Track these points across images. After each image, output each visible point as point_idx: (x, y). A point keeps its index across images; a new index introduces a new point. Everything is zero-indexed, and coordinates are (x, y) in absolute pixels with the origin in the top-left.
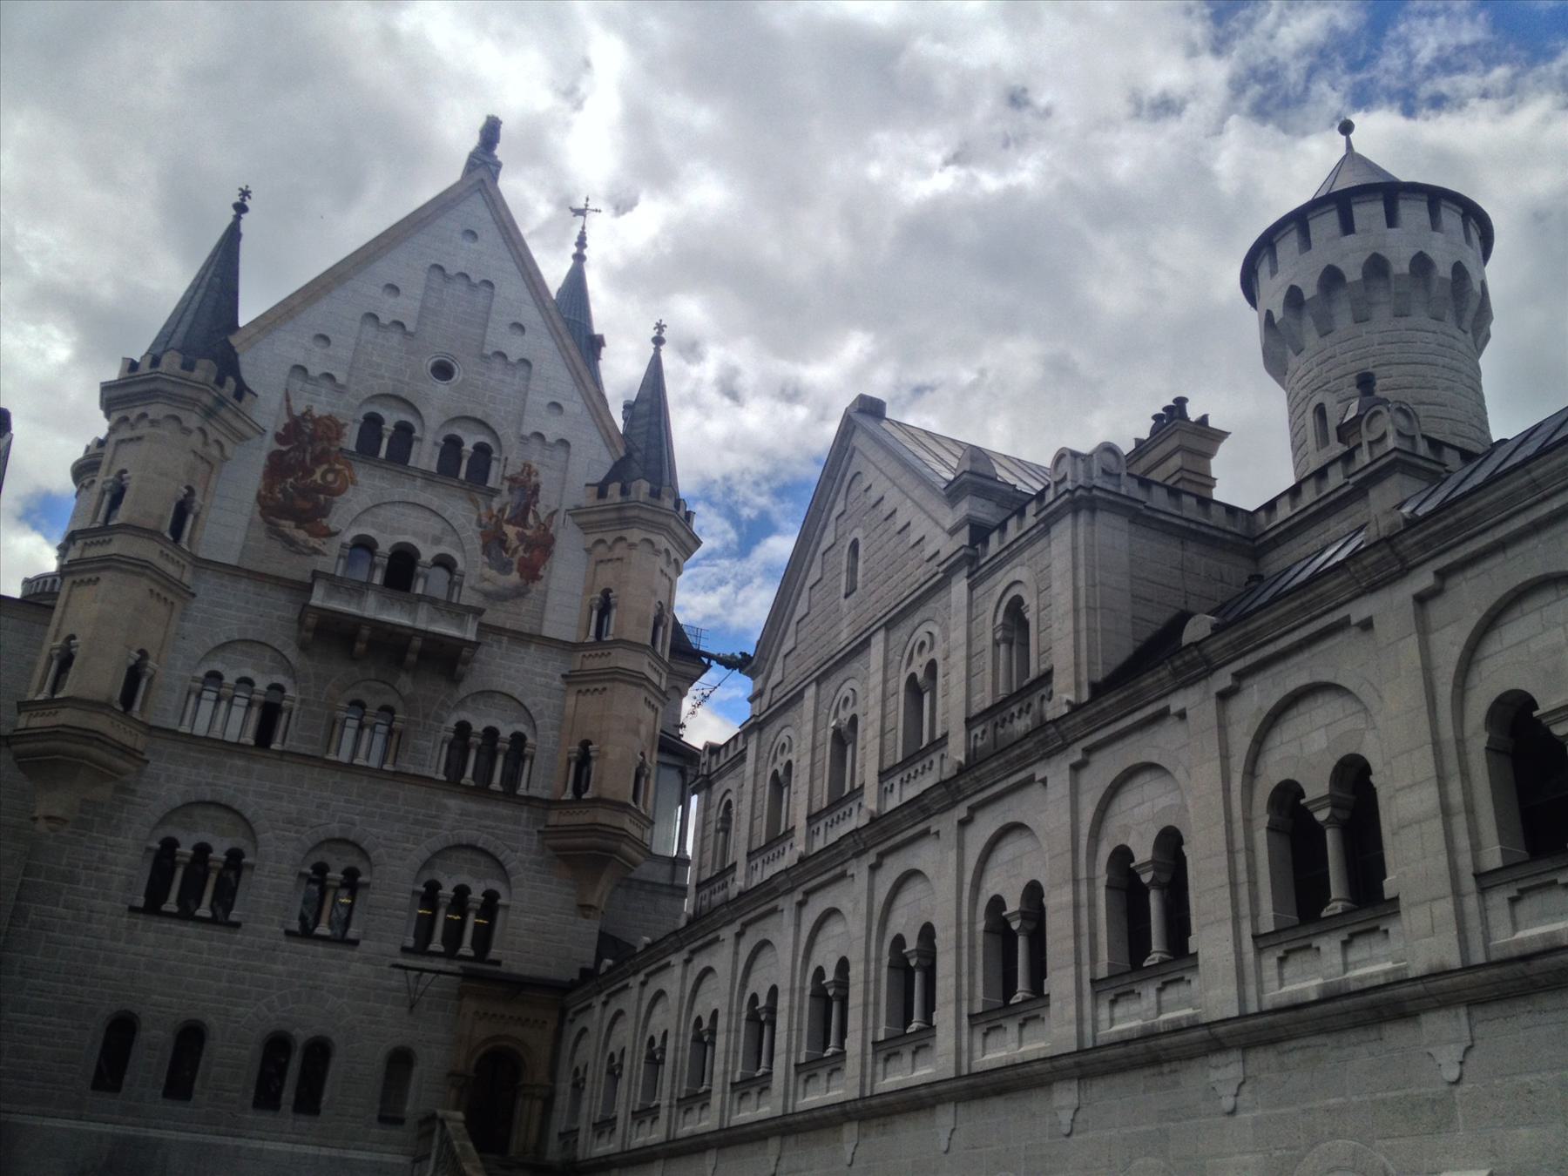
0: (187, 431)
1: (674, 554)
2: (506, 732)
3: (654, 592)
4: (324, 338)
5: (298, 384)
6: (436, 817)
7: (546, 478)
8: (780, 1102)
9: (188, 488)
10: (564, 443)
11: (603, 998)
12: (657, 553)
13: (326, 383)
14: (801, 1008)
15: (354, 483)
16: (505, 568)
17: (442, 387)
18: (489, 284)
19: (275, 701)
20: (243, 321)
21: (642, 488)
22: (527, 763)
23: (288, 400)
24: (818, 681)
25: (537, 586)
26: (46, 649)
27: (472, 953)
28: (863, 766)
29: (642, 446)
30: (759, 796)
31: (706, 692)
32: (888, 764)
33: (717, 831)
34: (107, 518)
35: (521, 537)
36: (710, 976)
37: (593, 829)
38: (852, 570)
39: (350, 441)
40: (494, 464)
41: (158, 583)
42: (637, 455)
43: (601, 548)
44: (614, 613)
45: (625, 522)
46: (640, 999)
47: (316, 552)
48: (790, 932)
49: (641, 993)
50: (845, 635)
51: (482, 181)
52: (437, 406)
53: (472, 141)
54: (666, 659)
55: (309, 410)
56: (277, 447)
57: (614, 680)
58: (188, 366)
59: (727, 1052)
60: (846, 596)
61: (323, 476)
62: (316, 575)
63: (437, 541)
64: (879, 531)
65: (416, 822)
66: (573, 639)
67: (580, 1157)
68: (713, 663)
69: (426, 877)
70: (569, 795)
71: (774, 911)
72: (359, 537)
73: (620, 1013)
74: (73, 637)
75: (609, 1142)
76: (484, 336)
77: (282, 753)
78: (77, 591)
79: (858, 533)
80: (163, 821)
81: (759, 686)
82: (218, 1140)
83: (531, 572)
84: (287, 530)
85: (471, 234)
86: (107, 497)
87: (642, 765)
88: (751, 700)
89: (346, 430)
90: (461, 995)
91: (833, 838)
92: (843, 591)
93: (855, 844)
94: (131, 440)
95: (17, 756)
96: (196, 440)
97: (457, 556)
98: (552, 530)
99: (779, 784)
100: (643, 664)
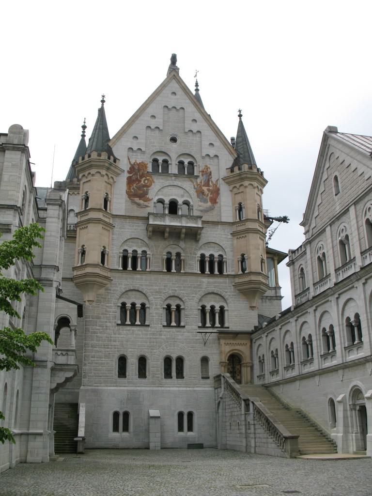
0: (103, 176)
1: (260, 187)
2: (216, 255)
3: (256, 201)
4: (136, 137)
5: (131, 154)
6: (200, 285)
8: (341, 359)
9: (106, 193)
10: (216, 156)
11: (266, 334)
12: (254, 188)
13: (139, 151)
14: (343, 330)
15: (154, 182)
16: (205, 201)
17: (174, 145)
18: (182, 108)
19: (135, 255)
20: (111, 137)
21: (245, 167)
22: (225, 264)
23: (129, 159)
24: (331, 225)
25: (217, 206)
26: (77, 250)
27: (220, 326)
28: (354, 251)
29: (242, 153)
30: (314, 265)
31: (273, 231)
32: (363, 250)
33: (299, 278)
34: (85, 208)
35: (209, 190)
36: (305, 324)
37: (250, 282)
38: (337, 186)
39: (150, 169)
40: (195, 168)
41: (105, 225)
42: (241, 156)
43: (235, 190)
44: (244, 210)
45: (243, 179)
46: (280, 334)
47: (147, 206)
48: (335, 308)
49: (280, 332)
50: (338, 209)
51: (174, 75)
52: (174, 152)
53: (169, 62)
54: (263, 222)
56: (129, 175)
57: (248, 233)
58: (99, 155)
59: (317, 346)
60: (336, 195)
61: (144, 182)
62: (149, 214)
63: (182, 196)
64: (345, 172)
65: (194, 287)
66: (232, 222)
67: (267, 383)
68: (274, 220)
69: (201, 304)
70: (240, 272)
71: (328, 301)
72: (158, 199)
73: (273, 338)
74: (84, 246)
75: (277, 377)
76: (184, 126)
77: (150, 271)
78: (82, 231)
79: (336, 173)
80: (120, 297)
81: (307, 229)
82: (157, 388)
83: (214, 201)
84: (137, 201)
85: (174, 93)
86: (84, 201)
87: (262, 259)
88: (305, 234)
89: (148, 165)
90: (219, 339)
91: (346, 276)
92: (334, 194)
93: (356, 277)
94: (87, 182)
95: (76, 284)
96: (106, 177)
97: (190, 200)
98: (218, 186)
99: (321, 260)
100: (256, 226)
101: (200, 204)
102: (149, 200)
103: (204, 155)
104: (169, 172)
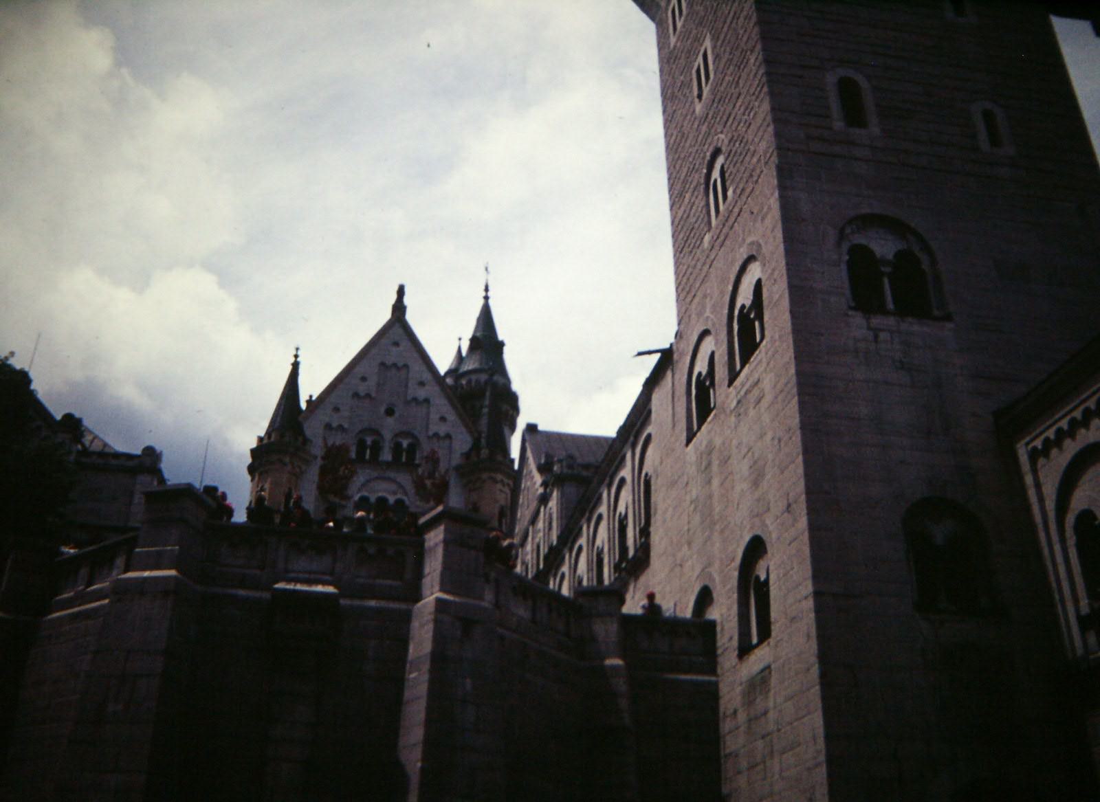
7: (441, 453)
12: (497, 482)
17: (390, 421)
35: (433, 484)
39: (353, 455)
53: (394, 297)
55: (334, 443)
63: (395, 493)
85: (396, 344)
96: (289, 468)
97: (405, 498)
101: (418, 503)
102: (348, 498)
103: (431, 433)
104: (381, 459)
